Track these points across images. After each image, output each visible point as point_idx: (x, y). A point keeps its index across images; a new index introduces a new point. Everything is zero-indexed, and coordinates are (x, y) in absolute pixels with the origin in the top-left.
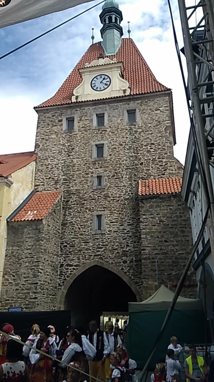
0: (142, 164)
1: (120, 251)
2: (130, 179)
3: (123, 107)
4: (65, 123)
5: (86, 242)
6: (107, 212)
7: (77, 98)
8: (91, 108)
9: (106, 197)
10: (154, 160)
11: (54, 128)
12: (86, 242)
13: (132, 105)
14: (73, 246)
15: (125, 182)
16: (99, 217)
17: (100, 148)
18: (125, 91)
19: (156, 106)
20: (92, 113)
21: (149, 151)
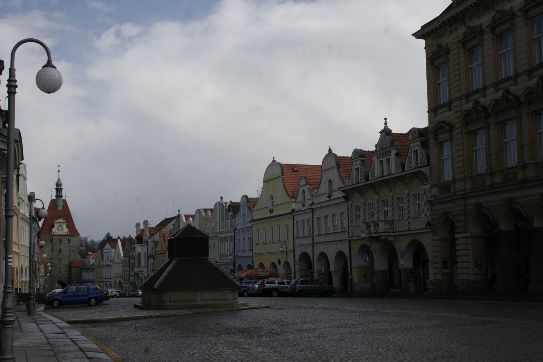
0: (71, 256)
1: (65, 278)
2: (68, 260)
3: (66, 238)
4: (50, 240)
5: (57, 275)
6: (62, 268)
7: (53, 232)
8: (58, 237)
9: (62, 264)
10: (74, 255)
11: (47, 242)
12: (57, 275)
13: (69, 238)
14: (54, 276)
15: (67, 261)
16: (60, 269)
17: (60, 250)
18: (67, 233)
19: (76, 239)
20: (57, 237)
21: (73, 253)
